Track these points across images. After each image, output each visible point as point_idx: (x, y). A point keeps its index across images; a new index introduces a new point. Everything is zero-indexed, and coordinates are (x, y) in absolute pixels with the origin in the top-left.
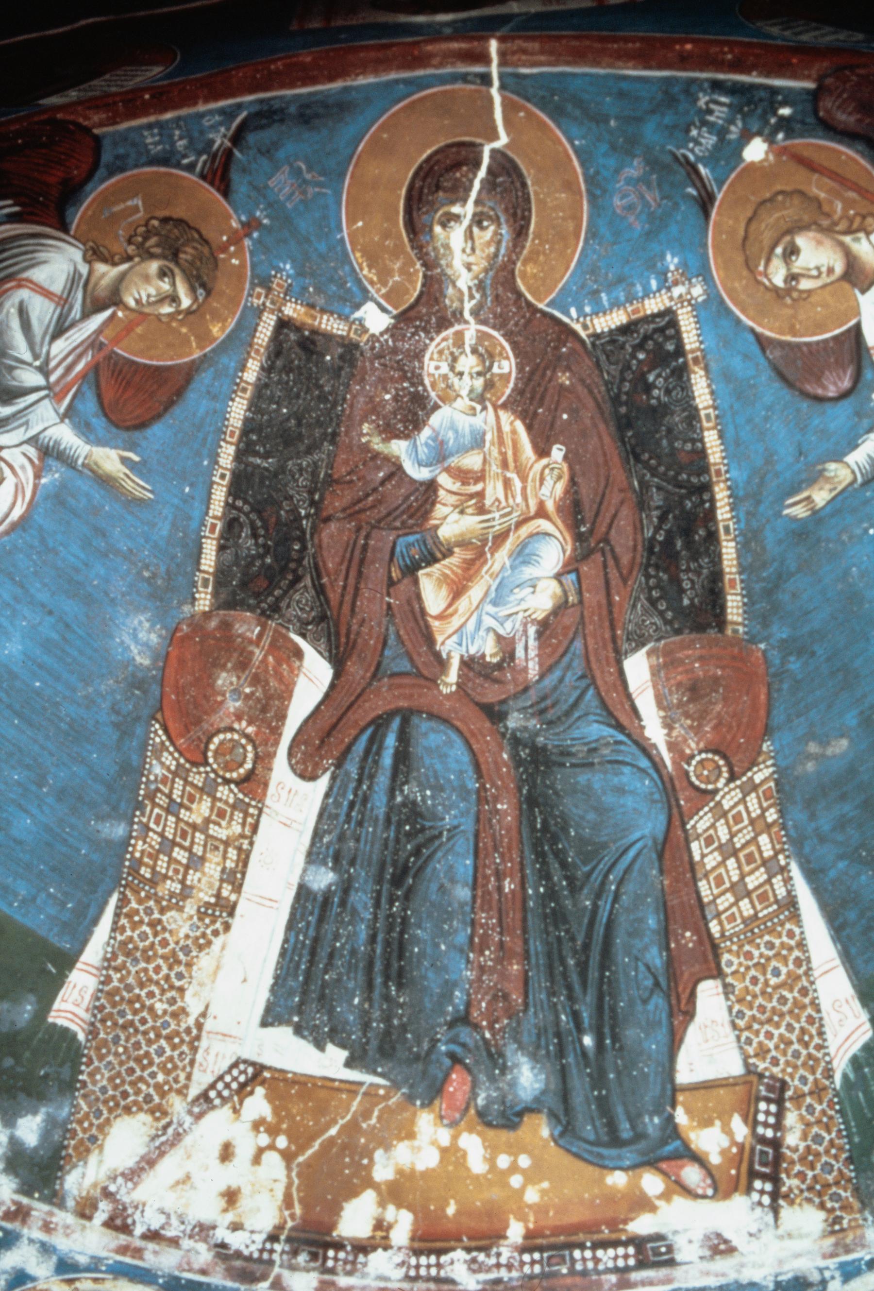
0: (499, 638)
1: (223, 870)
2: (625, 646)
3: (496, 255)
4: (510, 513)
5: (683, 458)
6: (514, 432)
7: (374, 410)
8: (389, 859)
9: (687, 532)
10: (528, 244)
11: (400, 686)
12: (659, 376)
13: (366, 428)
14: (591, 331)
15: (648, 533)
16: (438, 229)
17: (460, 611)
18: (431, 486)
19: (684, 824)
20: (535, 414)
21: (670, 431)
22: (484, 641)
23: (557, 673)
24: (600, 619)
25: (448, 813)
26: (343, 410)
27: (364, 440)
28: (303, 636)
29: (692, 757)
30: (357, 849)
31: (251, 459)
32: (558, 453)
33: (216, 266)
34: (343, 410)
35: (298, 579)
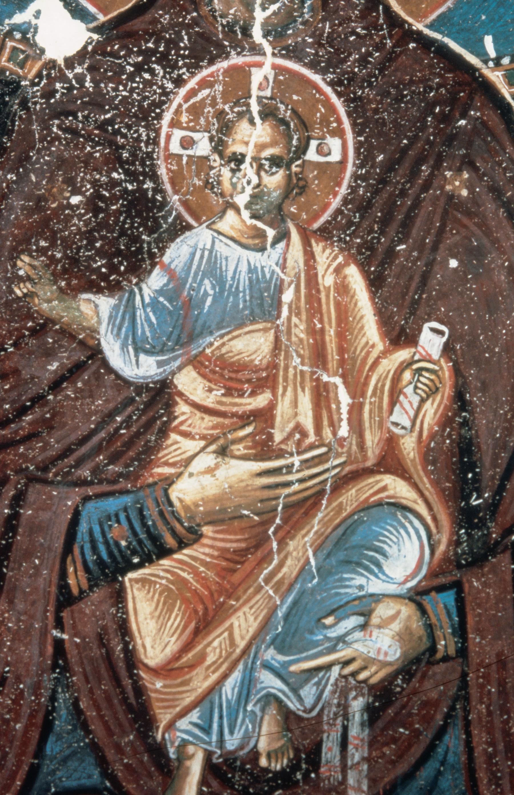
0: (288, 719)
4: (321, 459)
6: (343, 288)
7: (43, 228)
13: (24, 264)
17: (210, 659)
18: (161, 394)
20: (391, 254)
32: (431, 341)
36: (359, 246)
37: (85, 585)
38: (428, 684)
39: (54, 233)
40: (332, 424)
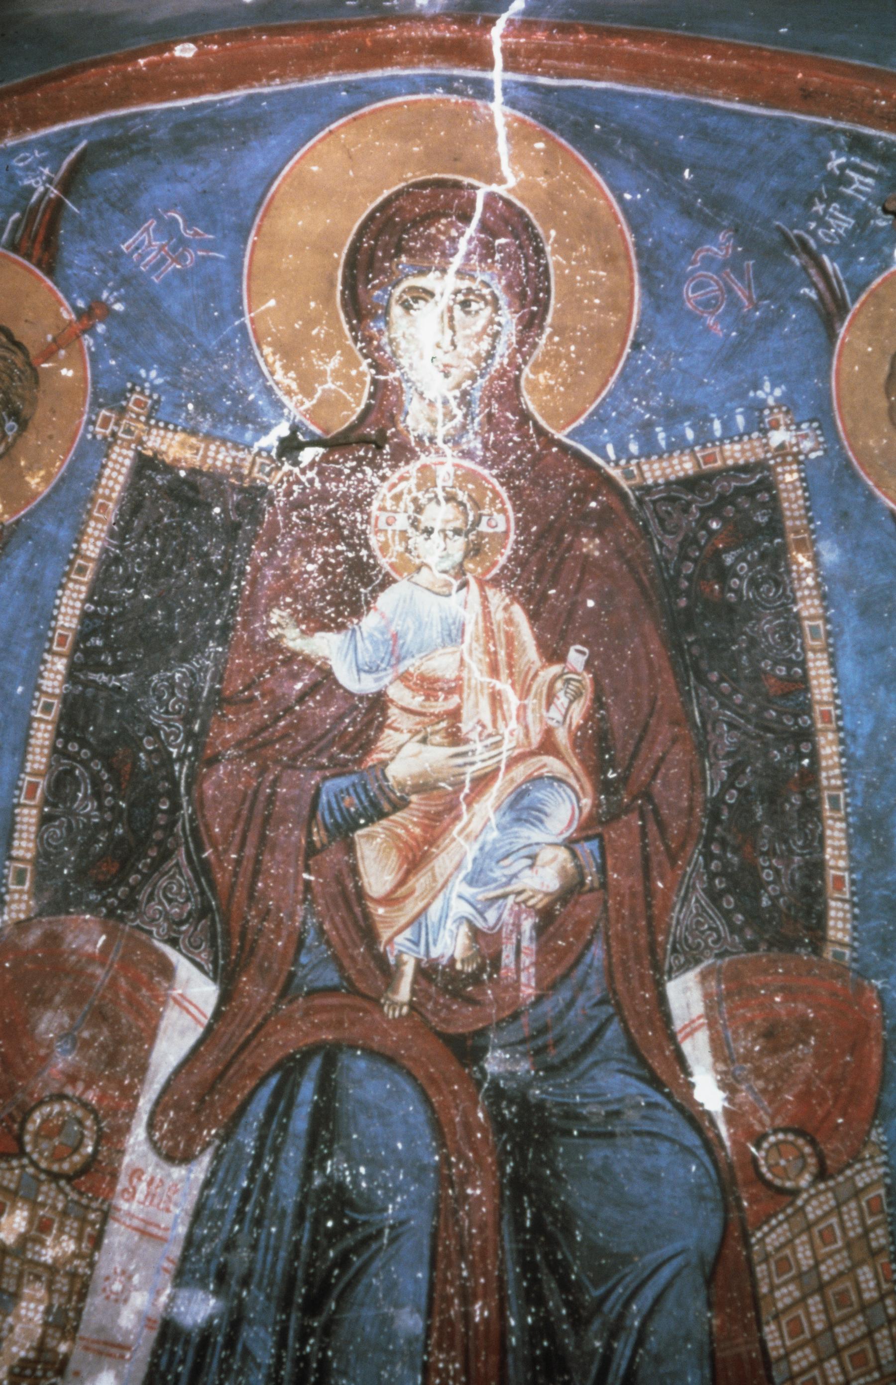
1: (48, 1311)
2: (669, 960)
3: (490, 355)
5: (771, 686)
6: (510, 621)
7: (288, 589)
8: (300, 1274)
9: (773, 797)
10: (542, 341)
11: (324, 1009)
12: (741, 558)
13: (275, 616)
14: (637, 480)
15: (712, 792)
16: (397, 311)
18: (378, 702)
19: (745, 1238)
20: (545, 597)
21: (753, 642)
22: (455, 937)
23: (563, 996)
24: (633, 914)
25: (392, 1200)
26: (240, 590)
27: (272, 634)
28: (173, 942)
29: (764, 1136)
30: (252, 1262)
31: (92, 676)
32: (576, 657)
33: (37, 382)
34: (240, 590)
35: (166, 855)
36: (521, 592)
37: (325, 841)
38: (578, 909)
39: (296, 591)
40: (504, 719)
